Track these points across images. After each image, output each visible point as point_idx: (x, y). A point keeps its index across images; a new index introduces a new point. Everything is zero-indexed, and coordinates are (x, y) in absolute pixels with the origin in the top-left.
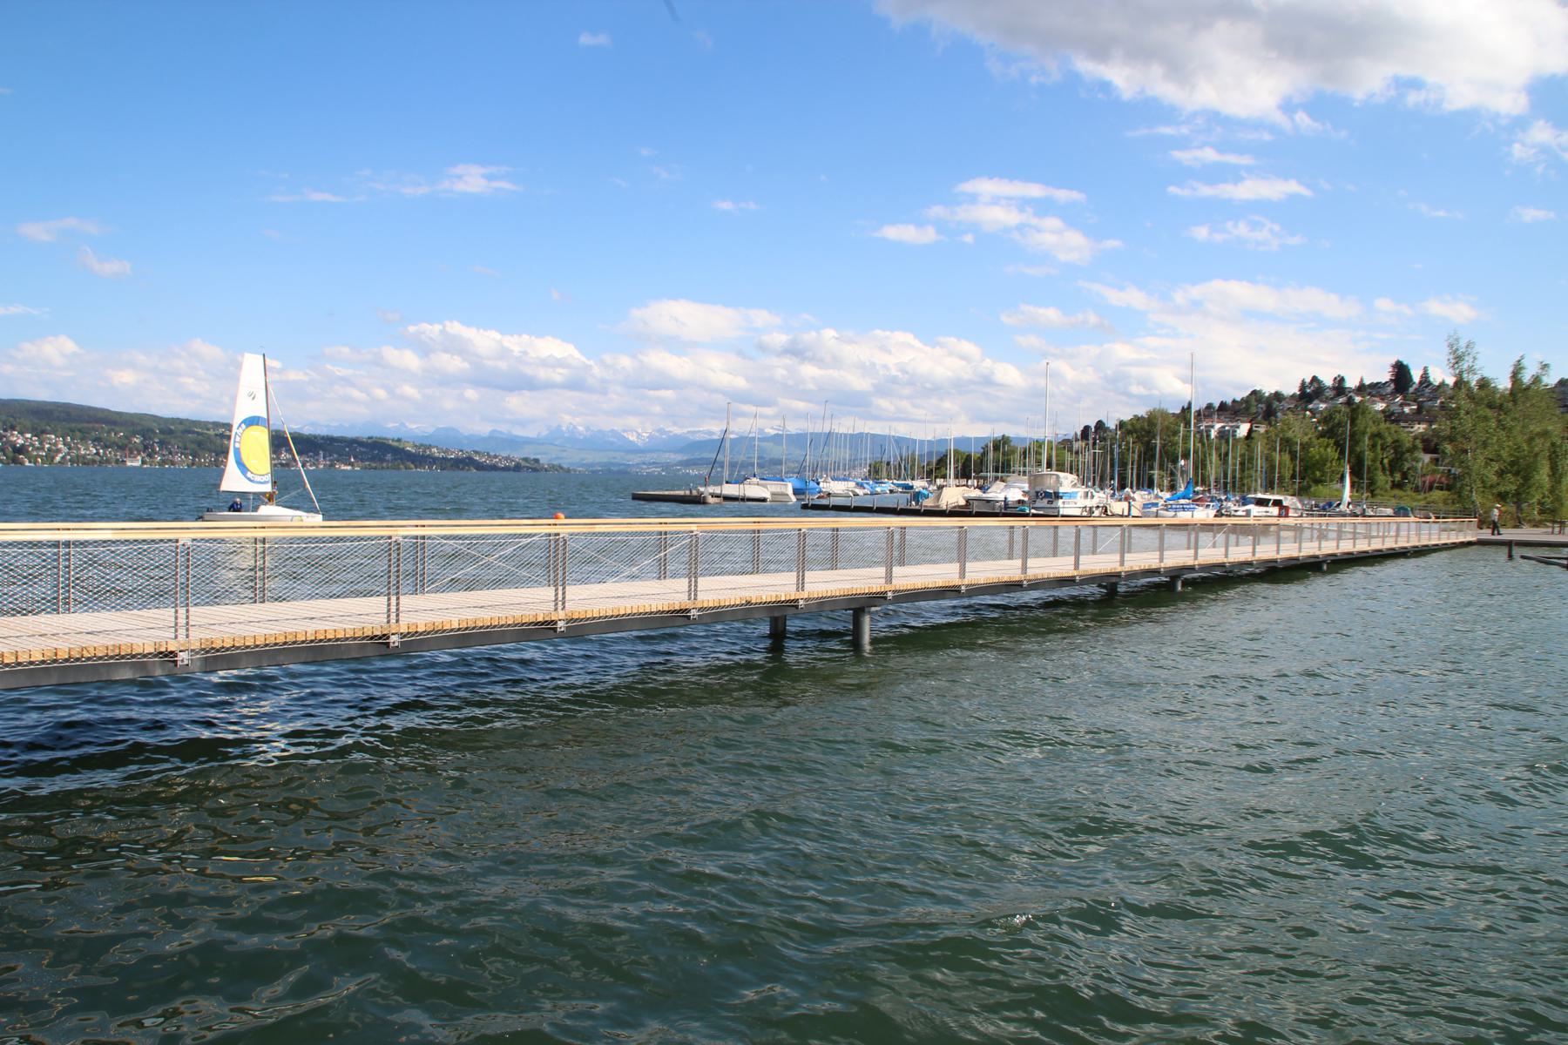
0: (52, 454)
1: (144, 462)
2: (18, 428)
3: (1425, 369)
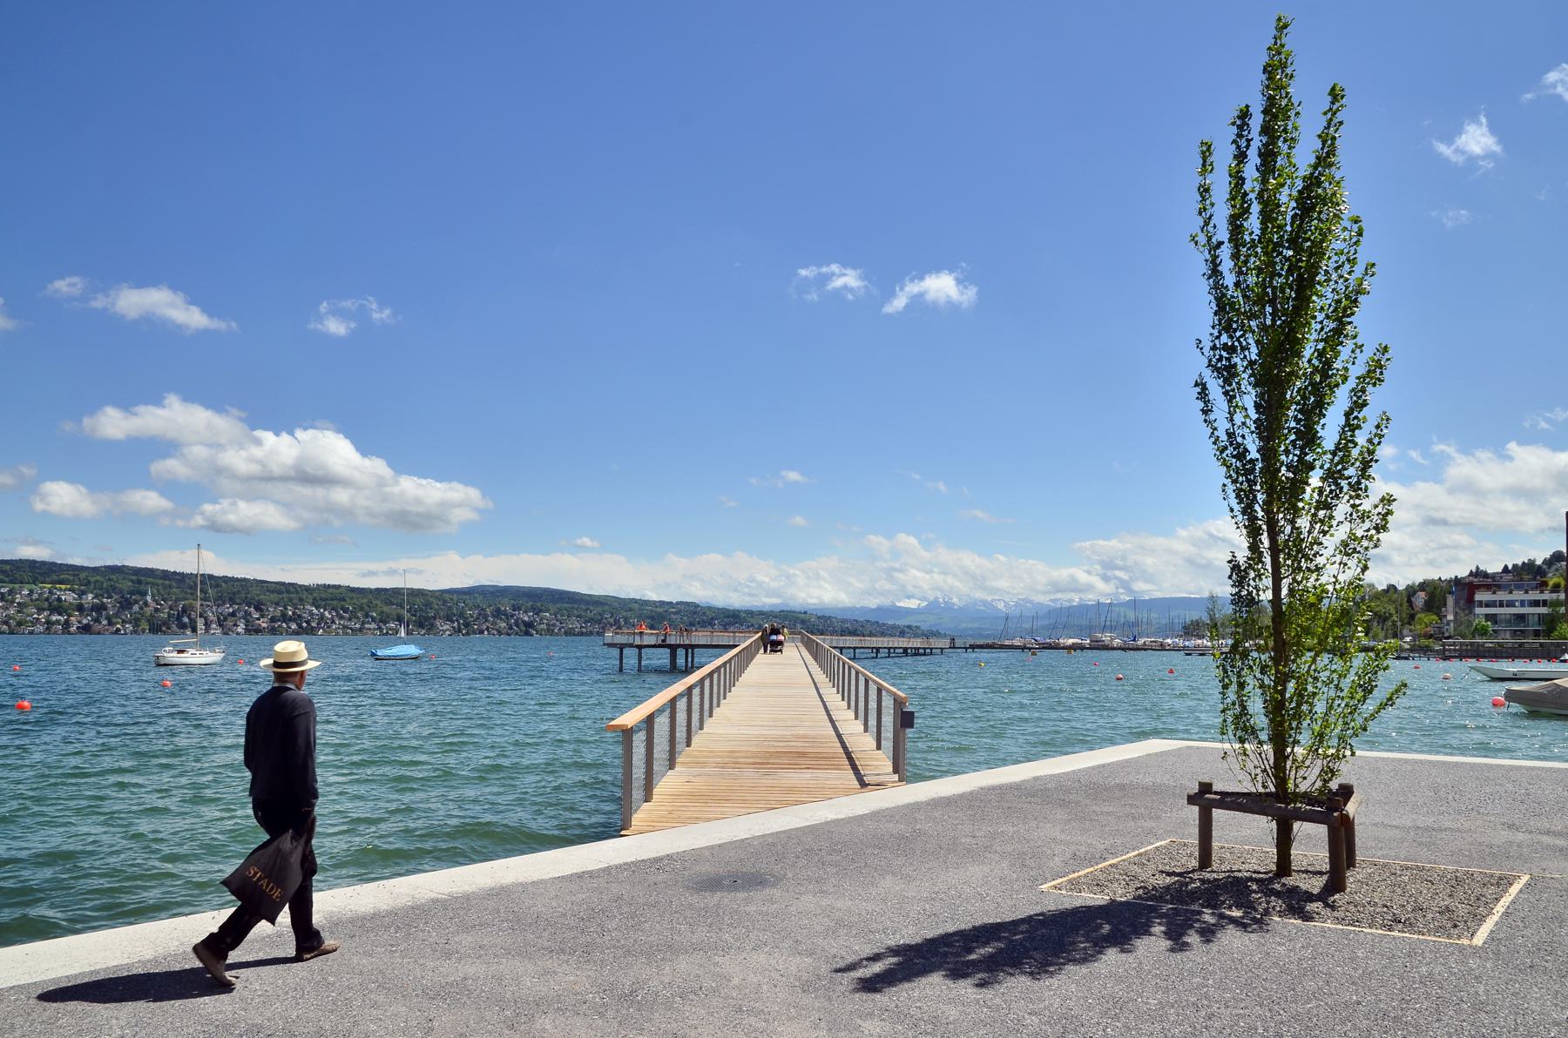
2: (523, 608)
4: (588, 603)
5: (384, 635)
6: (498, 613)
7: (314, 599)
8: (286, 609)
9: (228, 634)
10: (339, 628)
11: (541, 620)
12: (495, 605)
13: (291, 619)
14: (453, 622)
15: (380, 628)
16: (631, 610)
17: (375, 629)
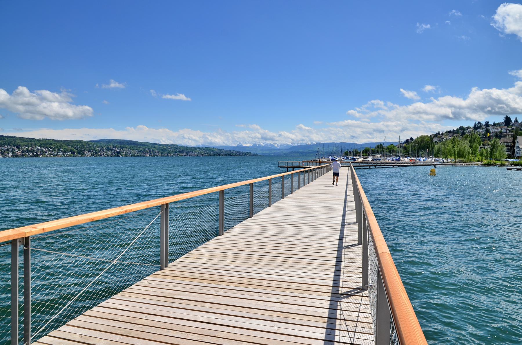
1: (149, 156)
2: (117, 147)
3: (516, 118)
4: (140, 145)
5: (65, 157)
6: (108, 149)
7: (41, 144)
8: (28, 147)
9: (5, 157)
10: (48, 155)
11: (123, 151)
12: (107, 146)
13: (30, 151)
14: (91, 152)
15: (64, 155)
17: (62, 155)
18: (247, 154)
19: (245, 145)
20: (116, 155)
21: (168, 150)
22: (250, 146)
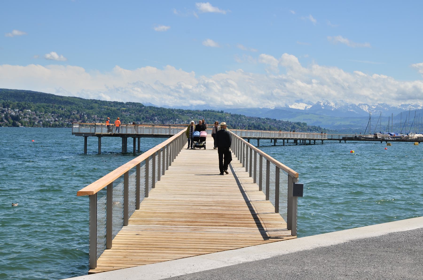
0: (33, 121)
2: (11, 106)
11: (25, 115)
16: (92, 108)
18: (297, 126)
19: (293, 107)
20: (10, 124)
21: (121, 116)
22: (305, 110)
